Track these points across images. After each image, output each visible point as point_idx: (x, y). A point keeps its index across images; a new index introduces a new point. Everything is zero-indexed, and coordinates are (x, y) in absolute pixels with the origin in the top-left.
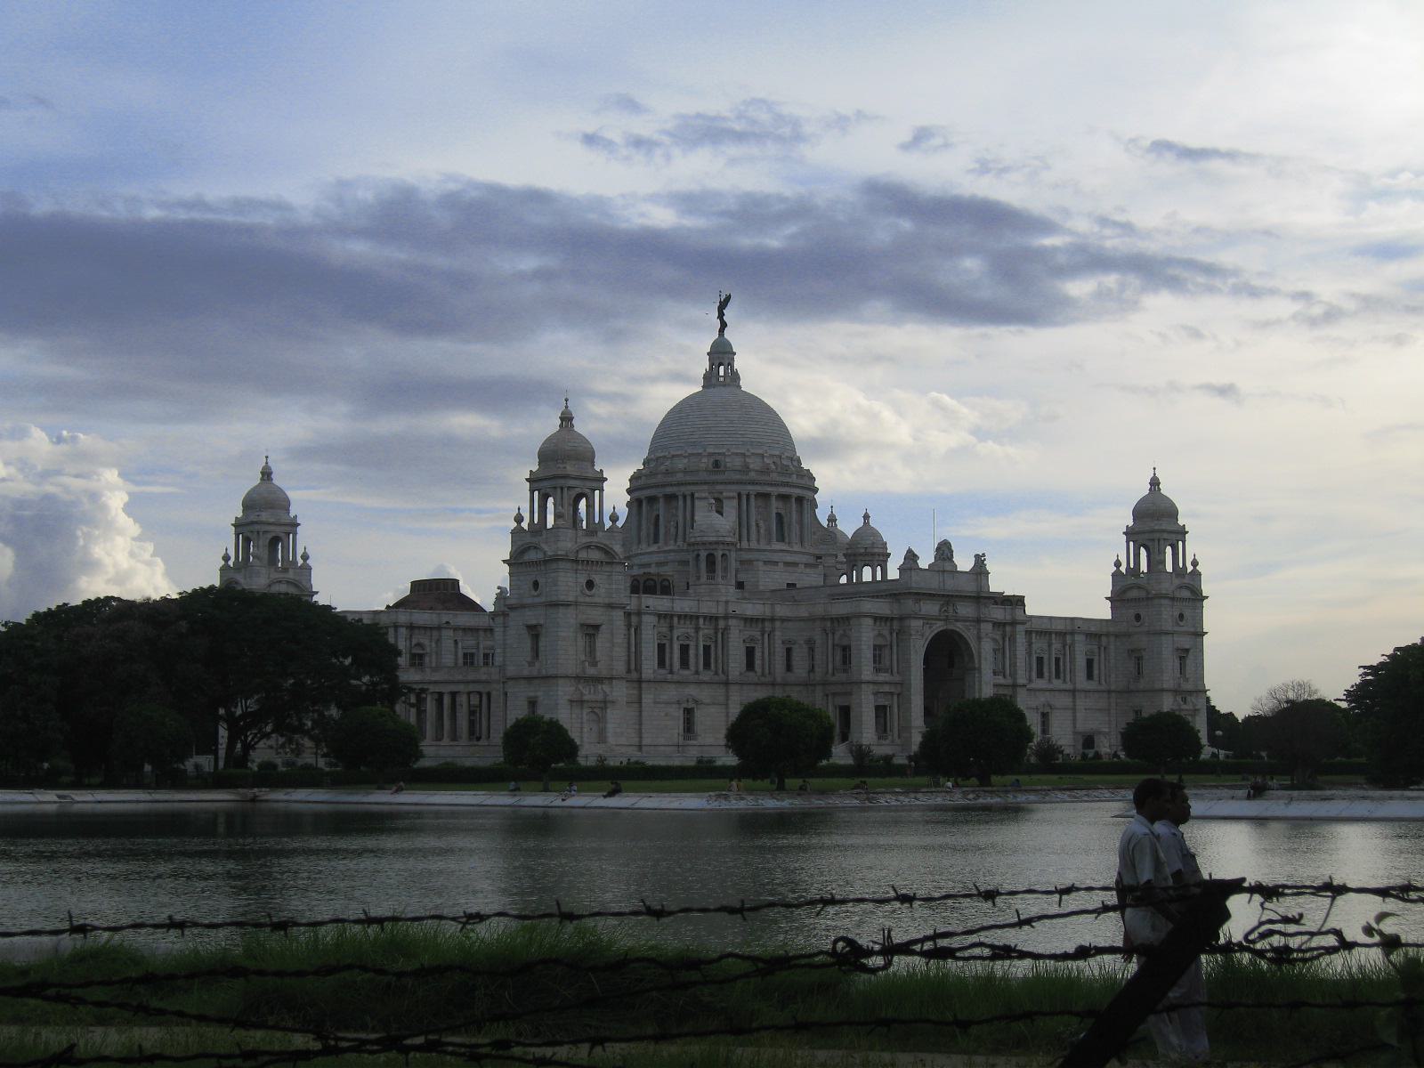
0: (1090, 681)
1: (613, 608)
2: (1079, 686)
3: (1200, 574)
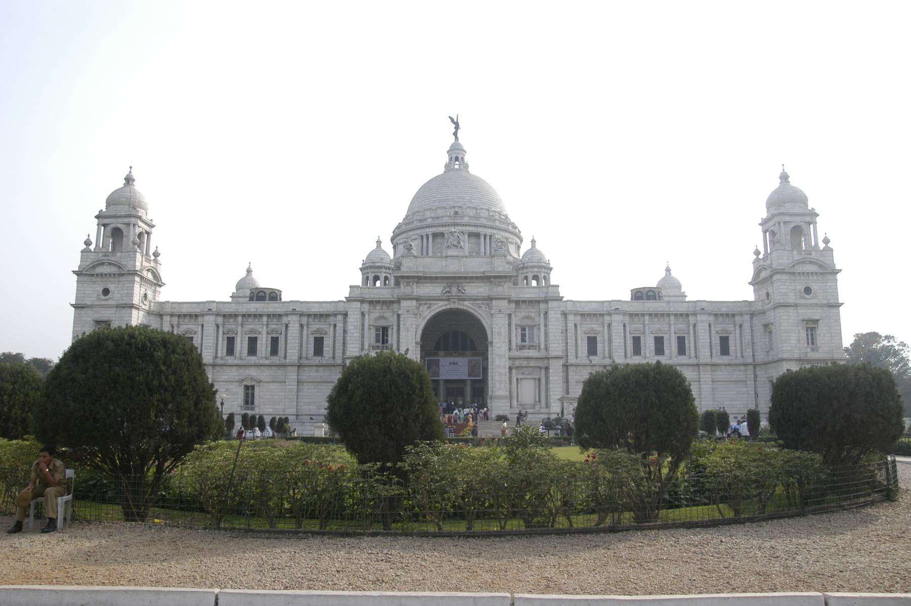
0: (725, 357)
1: (123, 307)
2: (702, 361)
3: (832, 250)
